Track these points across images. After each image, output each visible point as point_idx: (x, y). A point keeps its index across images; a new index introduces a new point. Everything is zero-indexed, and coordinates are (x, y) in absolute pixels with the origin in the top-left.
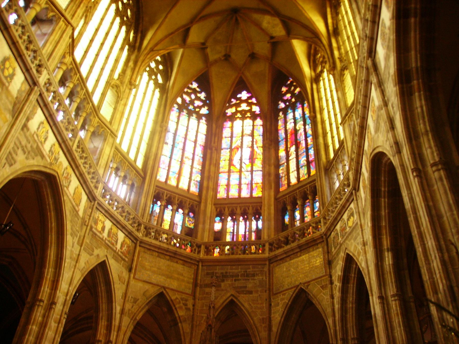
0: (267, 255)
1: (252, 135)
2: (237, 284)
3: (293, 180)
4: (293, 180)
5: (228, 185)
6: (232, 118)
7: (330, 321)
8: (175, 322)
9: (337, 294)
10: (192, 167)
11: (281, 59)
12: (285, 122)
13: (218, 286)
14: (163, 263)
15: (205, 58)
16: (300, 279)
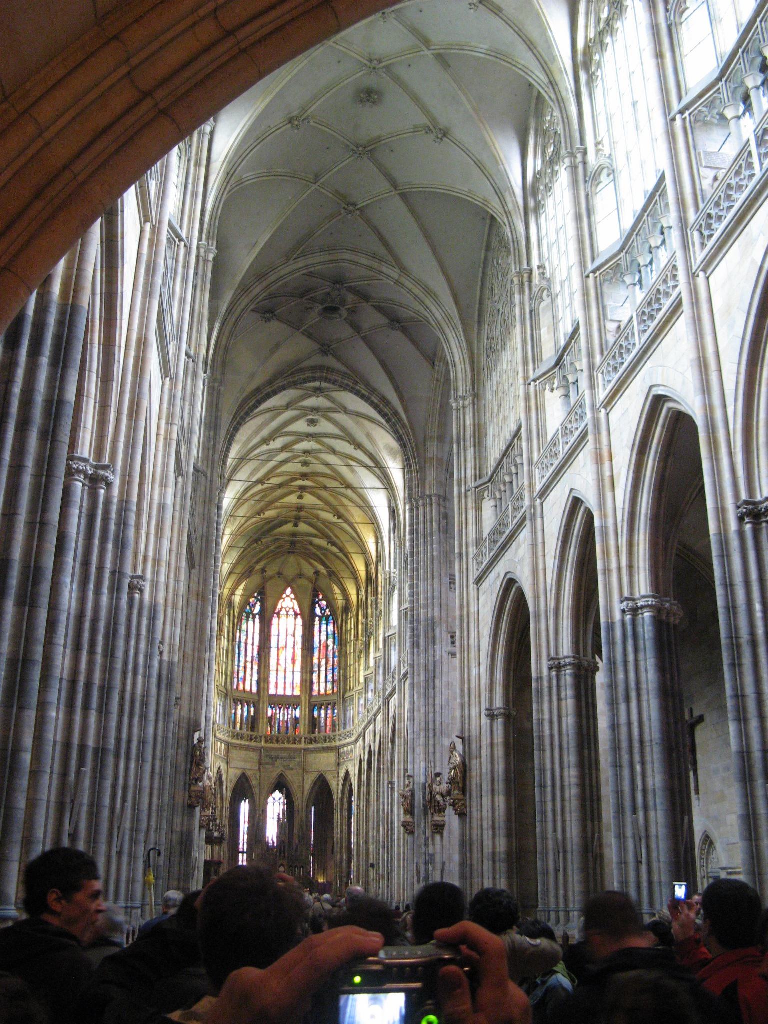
0: (303, 746)
1: (294, 636)
2: (285, 763)
3: (322, 692)
4: (322, 692)
5: (277, 683)
6: (278, 614)
7: (335, 797)
8: (251, 787)
9: (341, 786)
10: (252, 669)
11: (323, 582)
12: (320, 632)
13: (273, 764)
14: (243, 753)
15: (264, 578)
16: (323, 768)
